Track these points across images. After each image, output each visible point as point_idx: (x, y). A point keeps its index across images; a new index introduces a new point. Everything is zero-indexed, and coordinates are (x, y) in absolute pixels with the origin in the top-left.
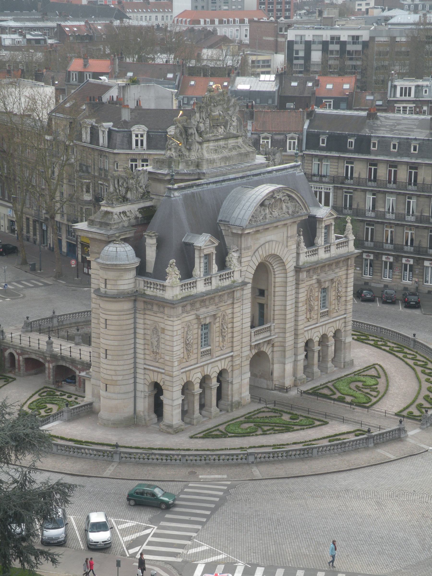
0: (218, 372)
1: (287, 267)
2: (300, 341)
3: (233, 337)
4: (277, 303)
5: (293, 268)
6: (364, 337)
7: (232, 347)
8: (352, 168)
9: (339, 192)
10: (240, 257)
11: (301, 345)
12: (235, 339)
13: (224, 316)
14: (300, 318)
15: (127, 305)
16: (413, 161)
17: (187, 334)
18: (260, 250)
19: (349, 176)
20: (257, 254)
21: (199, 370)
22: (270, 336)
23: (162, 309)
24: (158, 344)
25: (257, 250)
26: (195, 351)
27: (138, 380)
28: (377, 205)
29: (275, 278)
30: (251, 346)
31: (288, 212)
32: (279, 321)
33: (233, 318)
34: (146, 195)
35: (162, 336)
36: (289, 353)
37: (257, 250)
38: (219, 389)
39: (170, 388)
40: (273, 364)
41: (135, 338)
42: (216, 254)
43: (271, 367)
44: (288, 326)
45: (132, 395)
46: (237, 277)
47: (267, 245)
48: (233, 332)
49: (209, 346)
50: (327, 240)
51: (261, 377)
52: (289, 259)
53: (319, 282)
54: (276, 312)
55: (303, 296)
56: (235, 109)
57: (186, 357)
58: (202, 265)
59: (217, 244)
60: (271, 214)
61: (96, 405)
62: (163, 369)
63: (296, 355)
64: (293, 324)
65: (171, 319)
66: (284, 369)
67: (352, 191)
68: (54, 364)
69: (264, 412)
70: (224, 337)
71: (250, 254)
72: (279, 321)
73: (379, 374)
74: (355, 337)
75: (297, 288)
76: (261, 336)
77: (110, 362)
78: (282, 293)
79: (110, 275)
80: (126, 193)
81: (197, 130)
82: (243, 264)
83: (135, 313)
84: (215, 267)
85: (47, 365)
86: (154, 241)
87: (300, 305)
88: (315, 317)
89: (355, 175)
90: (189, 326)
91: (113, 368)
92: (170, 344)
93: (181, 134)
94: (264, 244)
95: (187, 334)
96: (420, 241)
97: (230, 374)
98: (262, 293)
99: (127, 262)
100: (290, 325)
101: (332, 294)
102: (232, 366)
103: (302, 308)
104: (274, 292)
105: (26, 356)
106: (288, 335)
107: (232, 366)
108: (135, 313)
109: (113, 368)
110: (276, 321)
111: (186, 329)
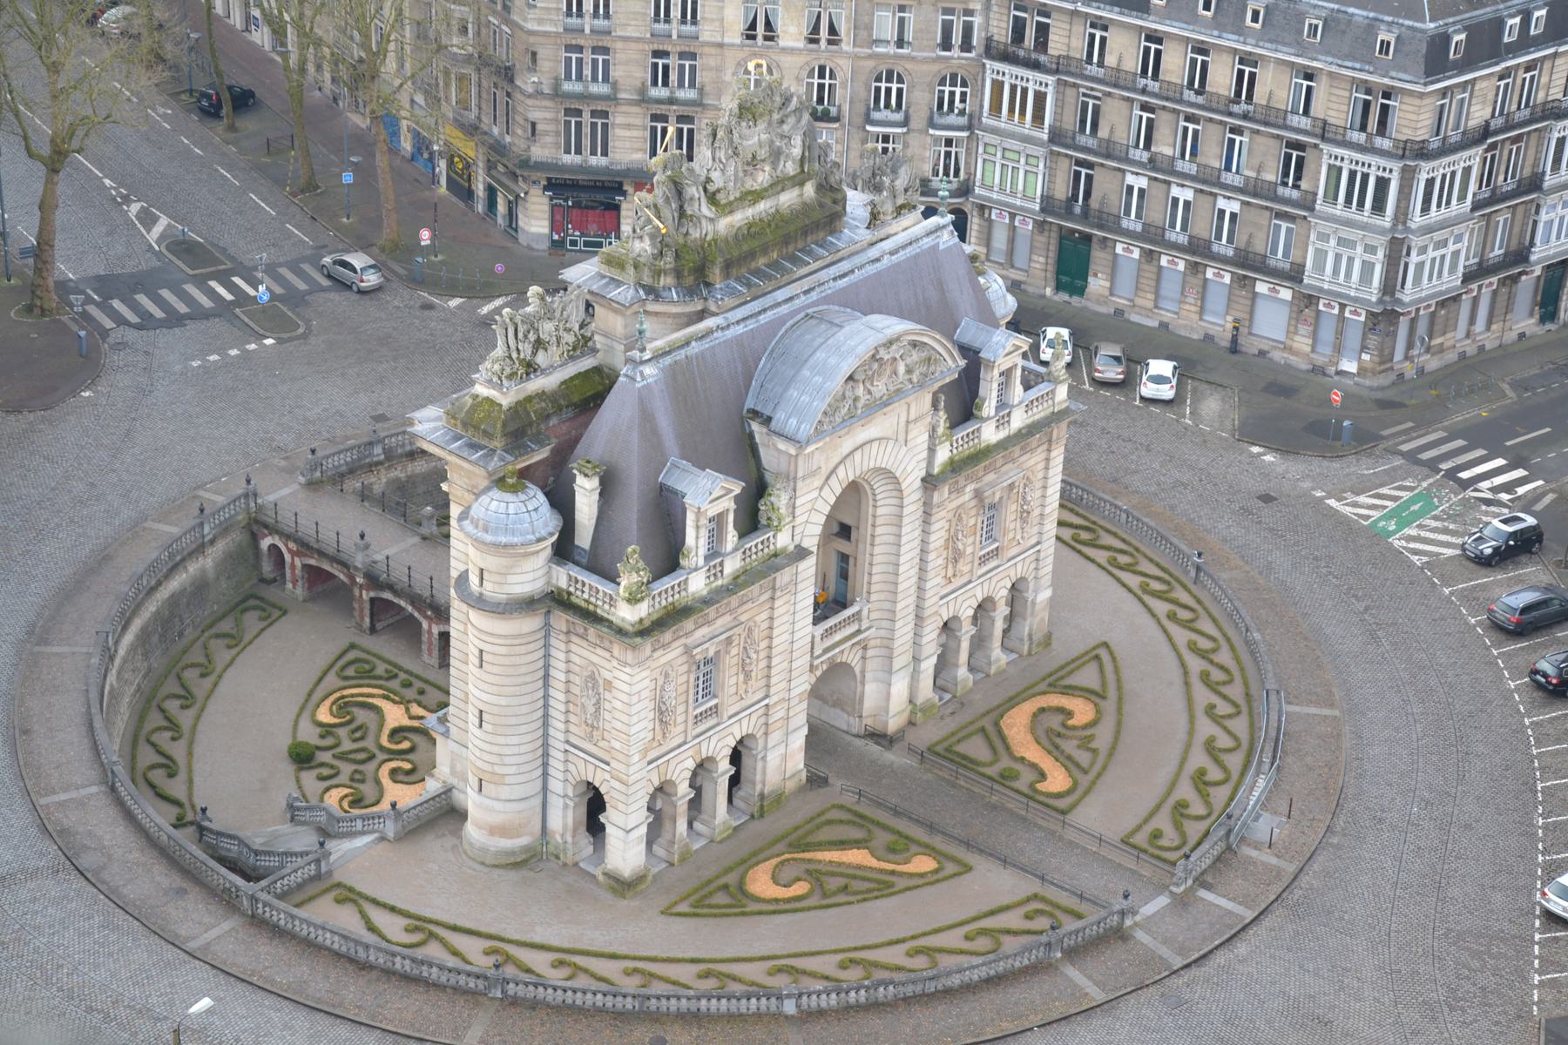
0: (733, 744)
1: (904, 486)
2: (927, 630)
3: (769, 667)
4: (876, 559)
5: (918, 483)
6: (1085, 535)
7: (768, 686)
8: (1103, 40)
9: (1070, 92)
10: (793, 498)
11: (931, 634)
12: (773, 671)
13: (750, 629)
14: (929, 585)
15: (530, 624)
16: (1248, 48)
17: (663, 689)
18: (841, 472)
19: (1095, 59)
20: (833, 481)
21: (690, 753)
22: (859, 632)
23: (607, 644)
24: (598, 710)
25: (833, 471)
26: (680, 719)
27: (551, 771)
28: (1156, 136)
29: (875, 506)
30: (811, 666)
31: (910, 381)
32: (883, 596)
33: (771, 628)
34: (584, 345)
35: (607, 695)
36: (901, 660)
37: (833, 471)
38: (735, 781)
39: (621, 807)
40: (863, 683)
41: (546, 685)
42: (735, 511)
43: (859, 689)
44: (899, 606)
45: (538, 801)
46: (783, 540)
47: (858, 455)
48: (769, 657)
49: (715, 696)
50: (1002, 405)
51: (837, 704)
52: (909, 469)
53: (978, 494)
54: (875, 579)
55: (938, 537)
56: (799, 121)
57: (659, 737)
58: (703, 542)
59: (737, 491)
60: (870, 392)
61: (457, 796)
62: (608, 764)
63: (916, 659)
64: (911, 600)
65: (628, 670)
66: (888, 694)
67: (1099, 95)
68: (372, 594)
69: (830, 822)
70: (748, 676)
71: (818, 482)
72: (883, 596)
73: (1104, 684)
74: (1067, 534)
75: (927, 515)
76: (838, 637)
77: (489, 738)
78: (891, 539)
79: (491, 562)
80: (534, 354)
81: (705, 190)
82: (798, 512)
83: (547, 636)
84: (731, 536)
85: (356, 592)
86: (594, 483)
87: (931, 556)
88: (966, 569)
89: (1110, 60)
90: (667, 675)
91: (495, 749)
92: (625, 718)
93: (667, 200)
94: (852, 453)
95: (663, 689)
96: (1251, 236)
97: (761, 742)
98: (845, 531)
99: (531, 537)
100: (906, 604)
101: (1011, 510)
102: (767, 724)
103: (936, 560)
104: (873, 536)
105: (312, 562)
106: (898, 624)
107: (767, 724)
108: (547, 636)
109: (495, 749)
110: (873, 597)
111: (660, 682)
